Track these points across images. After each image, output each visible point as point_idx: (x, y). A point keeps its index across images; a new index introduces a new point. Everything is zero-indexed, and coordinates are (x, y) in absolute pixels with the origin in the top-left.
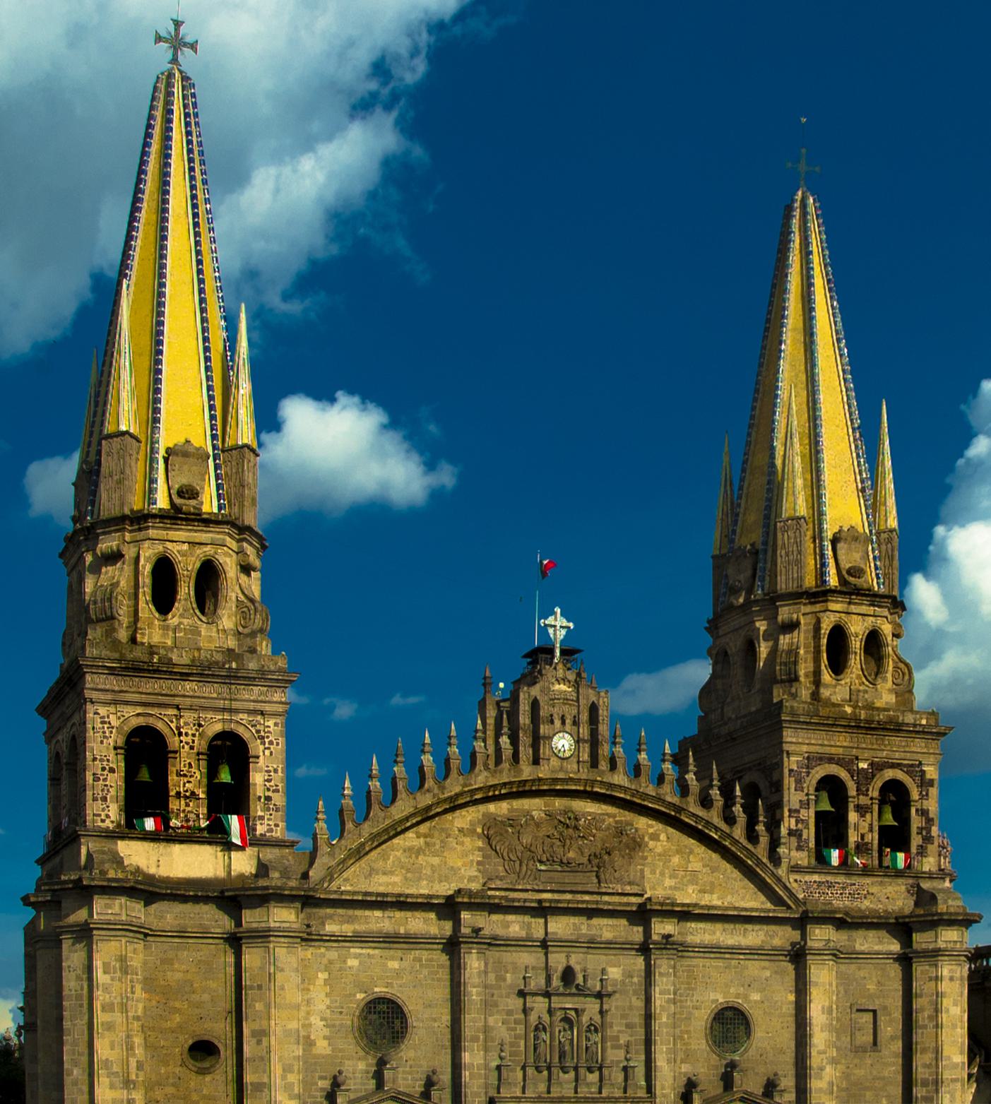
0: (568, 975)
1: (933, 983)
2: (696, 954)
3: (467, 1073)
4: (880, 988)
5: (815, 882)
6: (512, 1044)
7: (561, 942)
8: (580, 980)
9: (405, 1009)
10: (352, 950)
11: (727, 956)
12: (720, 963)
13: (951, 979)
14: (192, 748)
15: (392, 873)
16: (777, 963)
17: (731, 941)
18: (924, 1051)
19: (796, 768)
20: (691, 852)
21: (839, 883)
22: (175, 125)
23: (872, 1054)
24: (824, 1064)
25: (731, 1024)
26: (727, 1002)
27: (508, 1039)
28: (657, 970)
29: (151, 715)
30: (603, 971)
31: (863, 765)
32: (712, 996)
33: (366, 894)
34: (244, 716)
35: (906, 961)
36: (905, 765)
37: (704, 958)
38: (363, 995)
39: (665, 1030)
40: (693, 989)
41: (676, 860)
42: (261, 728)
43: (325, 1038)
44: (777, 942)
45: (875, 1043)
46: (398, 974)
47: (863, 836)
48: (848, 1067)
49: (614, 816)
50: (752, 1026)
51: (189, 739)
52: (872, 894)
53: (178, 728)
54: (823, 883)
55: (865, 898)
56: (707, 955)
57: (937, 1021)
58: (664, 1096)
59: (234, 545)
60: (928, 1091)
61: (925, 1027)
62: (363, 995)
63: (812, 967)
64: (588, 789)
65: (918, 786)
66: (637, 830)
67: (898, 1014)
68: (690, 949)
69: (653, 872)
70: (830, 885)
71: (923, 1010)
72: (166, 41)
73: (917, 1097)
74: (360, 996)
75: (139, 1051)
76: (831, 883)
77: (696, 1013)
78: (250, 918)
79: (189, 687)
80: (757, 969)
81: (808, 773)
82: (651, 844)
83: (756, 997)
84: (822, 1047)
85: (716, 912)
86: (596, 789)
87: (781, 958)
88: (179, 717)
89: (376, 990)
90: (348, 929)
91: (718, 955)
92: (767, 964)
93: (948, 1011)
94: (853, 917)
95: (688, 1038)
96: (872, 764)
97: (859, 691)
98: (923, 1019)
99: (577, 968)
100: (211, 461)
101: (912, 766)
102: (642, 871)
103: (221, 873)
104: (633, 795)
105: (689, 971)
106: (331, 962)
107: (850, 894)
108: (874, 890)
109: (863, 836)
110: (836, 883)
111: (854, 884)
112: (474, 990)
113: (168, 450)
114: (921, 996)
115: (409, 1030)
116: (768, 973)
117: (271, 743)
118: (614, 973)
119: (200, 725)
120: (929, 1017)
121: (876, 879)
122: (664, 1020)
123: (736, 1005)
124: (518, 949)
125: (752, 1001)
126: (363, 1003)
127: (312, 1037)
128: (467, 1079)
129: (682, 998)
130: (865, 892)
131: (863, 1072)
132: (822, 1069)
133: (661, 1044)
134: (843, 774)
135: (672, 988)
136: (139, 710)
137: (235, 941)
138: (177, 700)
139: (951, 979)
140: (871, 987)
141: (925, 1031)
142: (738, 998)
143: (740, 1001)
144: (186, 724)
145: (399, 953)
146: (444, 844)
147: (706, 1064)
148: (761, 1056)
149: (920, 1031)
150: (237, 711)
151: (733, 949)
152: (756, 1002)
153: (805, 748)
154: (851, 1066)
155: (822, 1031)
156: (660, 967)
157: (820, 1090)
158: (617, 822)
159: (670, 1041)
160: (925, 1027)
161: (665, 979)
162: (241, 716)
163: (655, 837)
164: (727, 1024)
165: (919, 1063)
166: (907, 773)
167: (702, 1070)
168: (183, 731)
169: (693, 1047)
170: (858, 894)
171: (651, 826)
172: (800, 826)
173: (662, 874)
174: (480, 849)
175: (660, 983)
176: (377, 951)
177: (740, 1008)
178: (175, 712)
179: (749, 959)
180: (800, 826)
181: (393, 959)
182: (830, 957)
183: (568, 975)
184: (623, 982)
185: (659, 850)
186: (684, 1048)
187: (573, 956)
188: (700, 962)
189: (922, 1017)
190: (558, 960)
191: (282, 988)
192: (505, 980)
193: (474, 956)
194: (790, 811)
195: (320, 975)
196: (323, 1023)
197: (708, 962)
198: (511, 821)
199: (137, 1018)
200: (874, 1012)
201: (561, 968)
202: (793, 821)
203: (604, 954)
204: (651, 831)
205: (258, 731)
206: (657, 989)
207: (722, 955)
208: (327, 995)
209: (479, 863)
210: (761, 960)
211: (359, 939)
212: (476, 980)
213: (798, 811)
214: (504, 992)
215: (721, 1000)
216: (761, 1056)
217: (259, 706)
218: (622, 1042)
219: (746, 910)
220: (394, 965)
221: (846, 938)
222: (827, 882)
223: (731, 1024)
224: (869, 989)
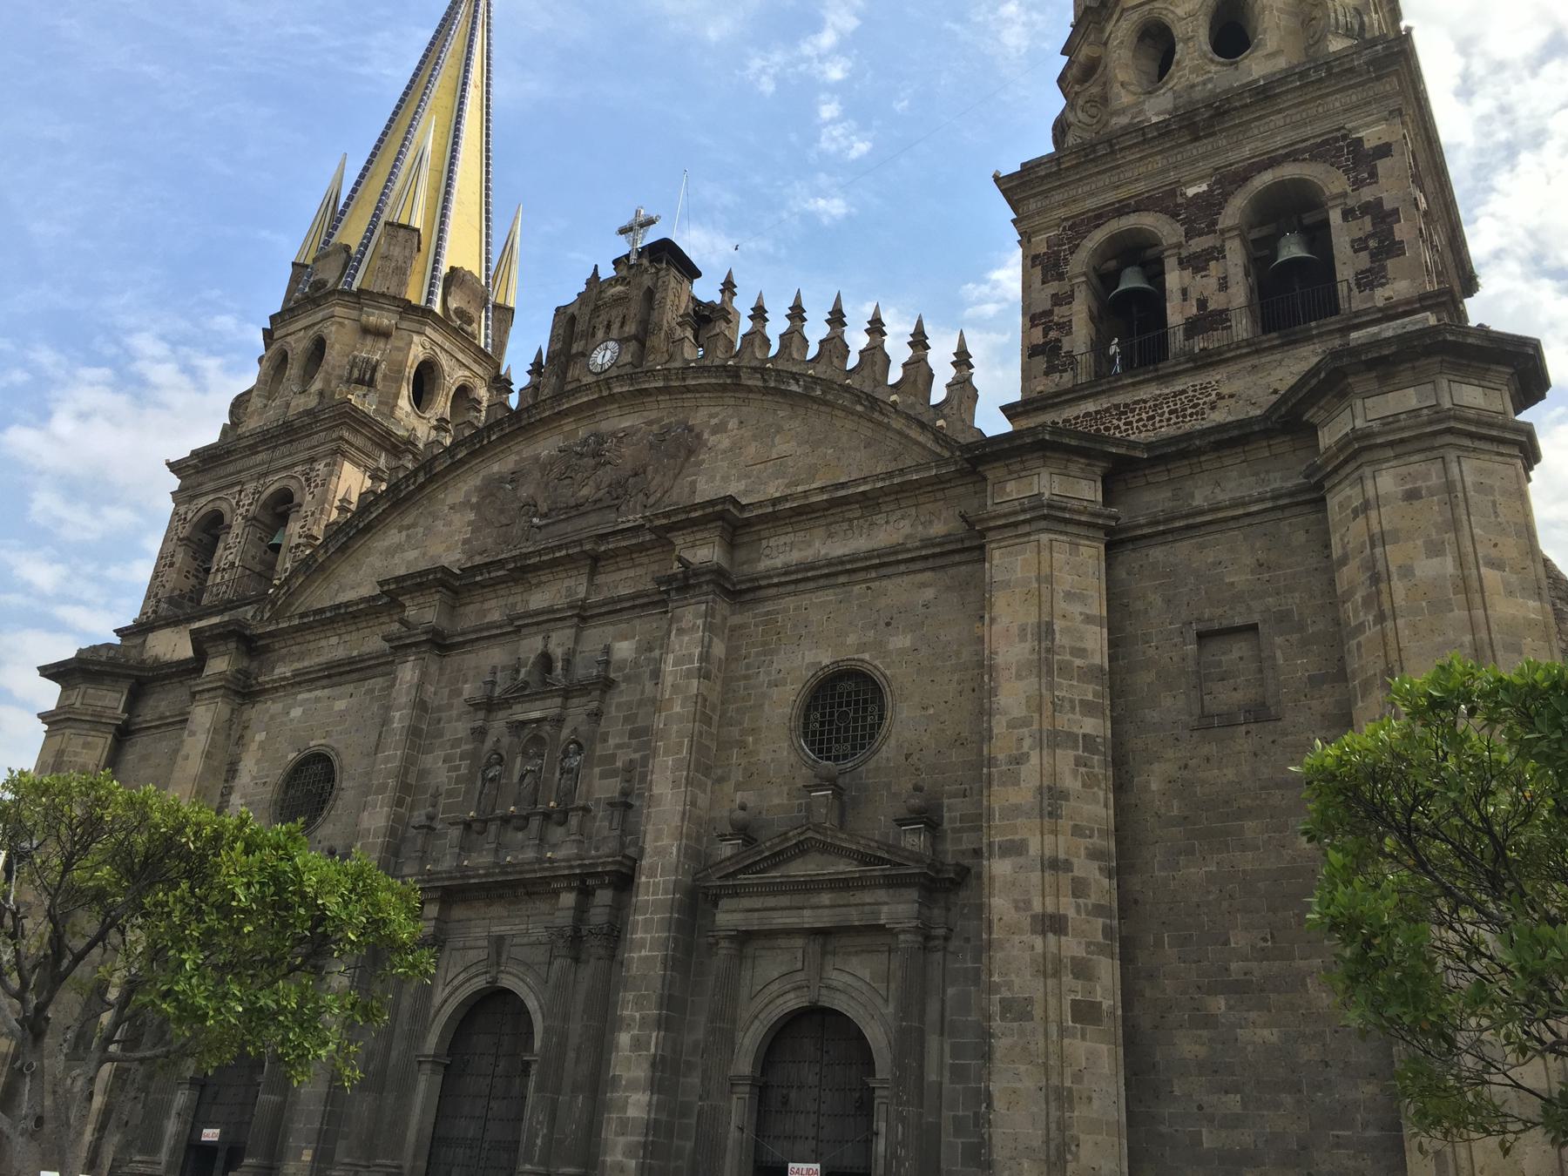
0: (546, 661)
1: (1361, 520)
2: (781, 590)
4: (1266, 576)
5: (1087, 414)
6: (450, 794)
7: (531, 616)
9: (336, 764)
10: (300, 697)
11: (842, 579)
12: (829, 596)
15: (359, 585)
16: (951, 571)
17: (839, 548)
20: (779, 430)
21: (1145, 402)
23: (1253, 726)
24: (1025, 749)
25: (843, 708)
27: (443, 789)
30: (607, 650)
32: (810, 657)
33: (302, 616)
36: (1304, 150)
37: (795, 594)
40: (772, 652)
41: (752, 450)
44: (938, 529)
46: (342, 715)
47: (1202, 304)
48: (1186, 766)
49: (662, 419)
50: (888, 700)
52: (1231, 396)
54: (1107, 410)
55: (1213, 408)
56: (801, 587)
58: (660, 852)
59: (354, 314)
61: (1360, 628)
63: (997, 553)
64: (605, 393)
65: (1346, 172)
68: (763, 583)
69: (712, 479)
71: (1350, 593)
74: (291, 756)
76: (1126, 405)
77: (775, 693)
79: (259, 458)
80: (898, 591)
82: (712, 440)
84: (1018, 712)
85: (788, 506)
86: (617, 390)
87: (957, 558)
89: (312, 744)
91: (822, 582)
92: (928, 575)
93: (1407, 572)
94: (1149, 446)
95: (756, 742)
97: (1193, 86)
98: (1356, 611)
99: (558, 652)
101: (1325, 142)
102: (693, 483)
104: (666, 378)
105: (766, 623)
106: (272, 718)
107: (1171, 412)
108: (1236, 386)
110: (1136, 402)
111: (1183, 392)
116: (929, 593)
120: (1367, 602)
121: (1233, 368)
122: (677, 709)
123: (859, 666)
124: (484, 644)
125: (893, 655)
130: (1213, 397)
131: (1230, 773)
132: (1019, 760)
133: (666, 753)
134: (1147, 221)
140: (1240, 578)
141: (1362, 638)
143: (867, 657)
145: (350, 688)
146: (428, 530)
147: (785, 789)
148: (907, 757)
151: (842, 563)
152: (902, 652)
153: (1062, 213)
154: (1192, 763)
155: (1019, 677)
156: (680, 620)
157: (1016, 810)
158: (662, 427)
159: (681, 744)
161: (686, 639)
163: (719, 429)
164: (840, 705)
166: (1313, 158)
167: (776, 801)
169: (762, 757)
170: (1195, 406)
171: (717, 414)
172: (1053, 334)
173: (726, 479)
174: (470, 523)
177: (865, 668)
179: (889, 577)
180: (1053, 334)
181: (340, 698)
182: (1043, 524)
184: (636, 662)
185: (725, 443)
186: (744, 762)
187: (554, 635)
188: (789, 602)
189: (1354, 612)
190: (531, 646)
192: (459, 693)
197: (805, 600)
198: (515, 477)
200: (1253, 628)
203: (611, 624)
204: (714, 421)
207: (832, 581)
208: (257, 762)
209: (465, 542)
210: (914, 572)
211: (303, 680)
213: (1051, 312)
214: (454, 713)
215: (826, 662)
216: (907, 757)
217: (312, 452)
218: (619, 764)
219: (843, 485)
221: (1169, 494)
222: (1117, 407)
223: (843, 708)
224: (1232, 584)
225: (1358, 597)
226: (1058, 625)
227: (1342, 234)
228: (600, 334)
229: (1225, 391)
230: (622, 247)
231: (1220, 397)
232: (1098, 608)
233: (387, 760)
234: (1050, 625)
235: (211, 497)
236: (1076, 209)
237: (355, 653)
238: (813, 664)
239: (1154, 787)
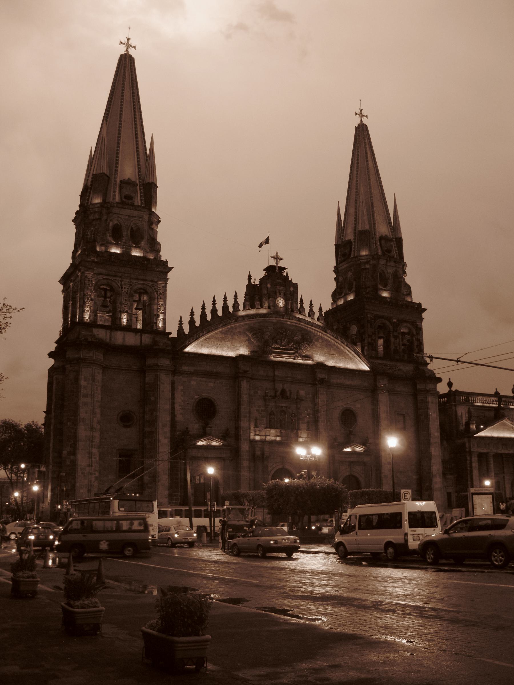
0: (283, 392)
8: (288, 394)
10: (193, 378)
13: (432, 403)
14: (127, 293)
17: (348, 382)
19: (369, 319)
22: (127, 72)
29: (109, 279)
30: (298, 392)
31: (395, 320)
34: (150, 283)
35: (415, 396)
38: (198, 397)
42: (156, 287)
43: (181, 414)
51: (126, 290)
53: (121, 285)
62: (198, 397)
66: (310, 337)
70: (385, 365)
72: (124, 44)
74: (196, 397)
75: (98, 416)
78: (150, 362)
81: (375, 322)
83: (358, 406)
88: (122, 281)
89: (203, 394)
90: (192, 369)
96: (398, 320)
99: (287, 390)
100: (138, 187)
103: (138, 343)
109: (396, 347)
112: (245, 396)
113: (121, 182)
117: (160, 294)
118: (302, 393)
119: (131, 285)
126: (197, 400)
127: (176, 413)
136: (105, 277)
137: (142, 372)
138: (121, 274)
139: (432, 403)
144: (125, 284)
150: (146, 280)
162: (148, 282)
168: (124, 287)
176: (204, 379)
178: (120, 279)
183: (283, 392)
190: (279, 386)
193: (245, 382)
194: (369, 335)
195: (179, 388)
196: (180, 407)
199: (98, 401)
200: (404, 415)
201: (280, 390)
202: (370, 339)
205: (155, 289)
206: (320, 400)
211: (197, 374)
220: (212, 385)
227: (416, 343)
228: (278, 294)
230: (273, 263)
235: (105, 277)
236: (378, 313)
237: (215, 370)
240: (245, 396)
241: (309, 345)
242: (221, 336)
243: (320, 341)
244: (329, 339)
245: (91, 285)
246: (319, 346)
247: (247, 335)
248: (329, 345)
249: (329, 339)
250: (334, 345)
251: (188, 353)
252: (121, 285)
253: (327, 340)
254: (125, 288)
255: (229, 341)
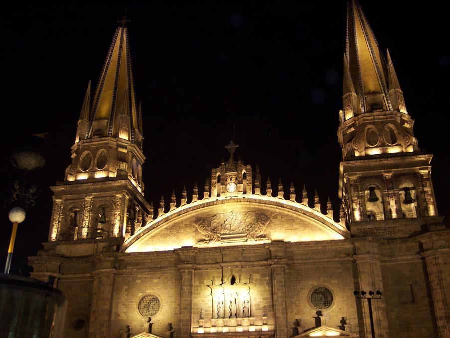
1: (435, 266)
3: (181, 323)
18: (438, 301)
19: (353, 183)
26: (319, 285)
28: (275, 272)
29: (75, 202)
39: (280, 299)
45: (413, 300)
48: (399, 313)
52: (401, 230)
55: (398, 232)
57: (440, 285)
60: (443, 322)
61: (436, 289)
67: (424, 285)
73: (439, 327)
95: (299, 303)
111: (390, 227)
112: (185, 288)
114: (431, 274)
115: (161, 306)
116: (341, 270)
117: (118, 205)
126: (141, 297)
128: (181, 326)
129: (295, 285)
130: (397, 230)
133: (279, 305)
135: (283, 280)
136: (71, 201)
142: (325, 283)
143: (326, 284)
149: (434, 291)
159: (283, 304)
160: (436, 289)
161: (279, 276)
165: (437, 308)
175: (277, 278)
177: (327, 287)
191: (103, 292)
206: (276, 281)
212: (187, 283)
225: (435, 282)
226: (376, 282)
229: (400, 229)
231: (399, 230)
232: (381, 279)
233: (185, 300)
234: (374, 282)
238: (311, 285)
239: (393, 317)
240: (185, 288)
241: (263, 224)
242: (166, 232)
243: (279, 217)
244: (289, 213)
245: (59, 210)
246: (278, 223)
247: (194, 227)
248: (291, 219)
249: (289, 213)
250: (297, 218)
251: (130, 254)
252: (85, 205)
253: (288, 215)
254: (87, 207)
255: (174, 235)
